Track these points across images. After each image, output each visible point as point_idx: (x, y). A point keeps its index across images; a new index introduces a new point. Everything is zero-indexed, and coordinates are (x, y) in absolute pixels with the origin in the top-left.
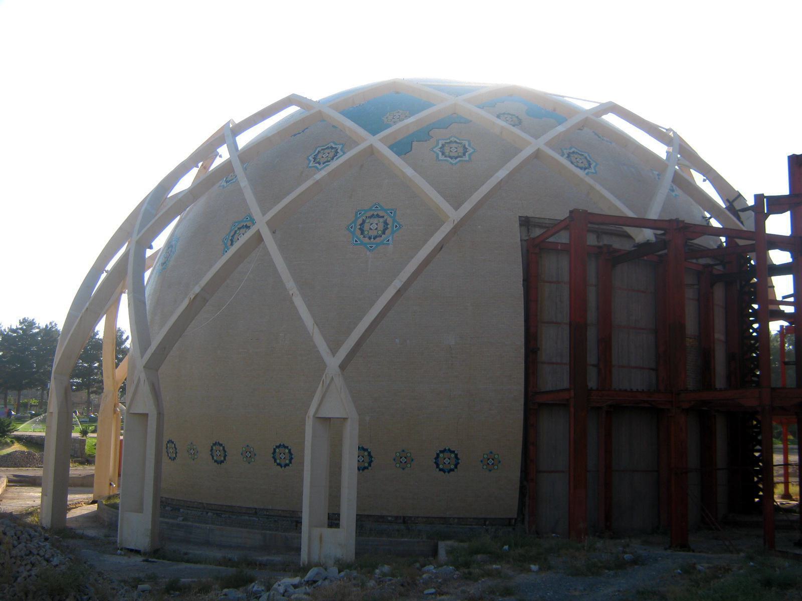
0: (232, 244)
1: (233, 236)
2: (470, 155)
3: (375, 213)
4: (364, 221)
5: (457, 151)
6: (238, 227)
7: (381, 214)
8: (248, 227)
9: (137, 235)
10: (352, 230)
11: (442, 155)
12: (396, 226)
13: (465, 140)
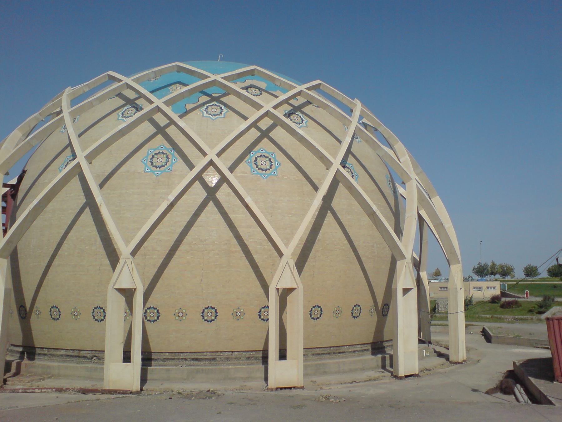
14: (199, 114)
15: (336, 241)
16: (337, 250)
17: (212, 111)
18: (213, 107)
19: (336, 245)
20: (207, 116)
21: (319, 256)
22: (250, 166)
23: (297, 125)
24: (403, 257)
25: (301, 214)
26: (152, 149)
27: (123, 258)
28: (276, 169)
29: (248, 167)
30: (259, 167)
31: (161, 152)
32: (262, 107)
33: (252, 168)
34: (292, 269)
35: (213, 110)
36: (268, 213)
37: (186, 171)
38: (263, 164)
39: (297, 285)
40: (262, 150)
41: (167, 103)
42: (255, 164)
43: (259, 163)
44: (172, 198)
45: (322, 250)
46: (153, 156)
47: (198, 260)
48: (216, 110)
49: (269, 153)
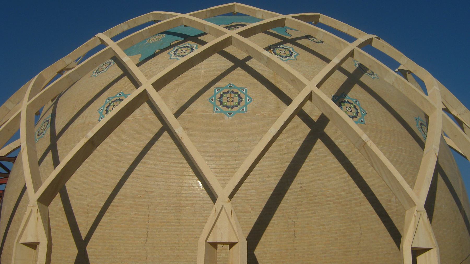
0: (107, 112)
1: (108, 107)
2: (295, 56)
3: (230, 90)
4: (222, 96)
5: (285, 53)
6: (112, 100)
7: (235, 91)
8: (120, 100)
9: (28, 101)
10: (213, 102)
11: (275, 54)
12: (249, 100)
13: (290, 47)
14: (166, 57)
15: (328, 192)
16: (329, 204)
17: (181, 53)
18: (182, 49)
19: (328, 197)
20: (174, 57)
21: (302, 211)
22: (213, 104)
23: (282, 58)
24: (412, 204)
25: (277, 157)
26: (110, 98)
27: (30, 206)
28: (246, 106)
29: (210, 104)
30: (225, 104)
31: (118, 98)
32: (225, 33)
33: (215, 105)
34: (230, 216)
35: (182, 52)
36: (231, 157)
37: (139, 115)
38: (230, 101)
39: (237, 238)
40: (231, 86)
41: (115, 39)
42: (219, 101)
43: (224, 99)
44: (90, 134)
45: (306, 203)
46: (110, 104)
47: (143, 216)
48: (185, 51)
49: (239, 89)
